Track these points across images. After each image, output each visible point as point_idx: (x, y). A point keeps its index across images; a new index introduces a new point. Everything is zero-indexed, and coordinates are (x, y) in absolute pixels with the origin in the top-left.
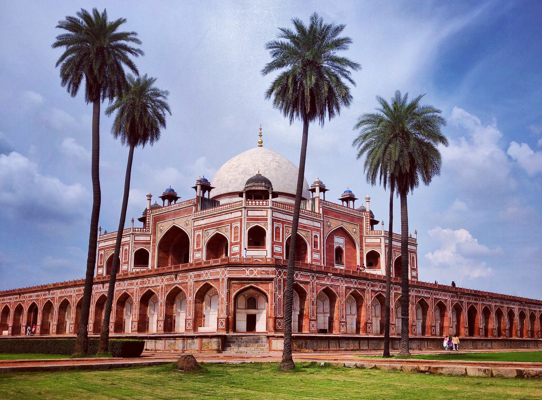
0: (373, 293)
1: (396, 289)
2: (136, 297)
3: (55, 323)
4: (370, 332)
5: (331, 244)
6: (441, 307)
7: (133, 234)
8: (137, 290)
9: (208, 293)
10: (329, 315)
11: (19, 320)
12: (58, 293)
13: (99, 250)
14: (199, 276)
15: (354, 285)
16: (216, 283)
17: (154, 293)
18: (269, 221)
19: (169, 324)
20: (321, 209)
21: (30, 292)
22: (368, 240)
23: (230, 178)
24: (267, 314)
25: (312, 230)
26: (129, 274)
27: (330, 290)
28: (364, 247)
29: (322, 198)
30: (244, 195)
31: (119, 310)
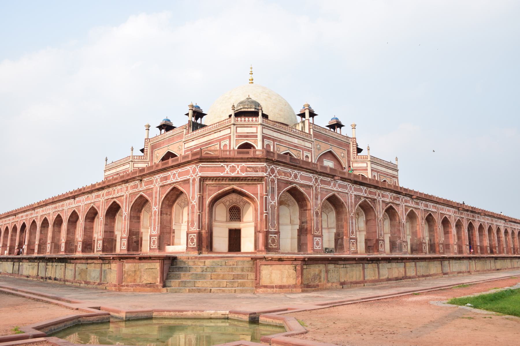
0: (384, 205)
2: (102, 210)
4: (382, 251)
7: (132, 161)
8: (103, 202)
10: (335, 231)
12: (40, 213)
14: (166, 178)
15: (364, 192)
16: (187, 185)
18: (260, 138)
20: (311, 130)
21: (22, 212)
22: (355, 165)
24: (256, 228)
25: (304, 150)
26: (97, 185)
29: (311, 121)
31: (88, 227)
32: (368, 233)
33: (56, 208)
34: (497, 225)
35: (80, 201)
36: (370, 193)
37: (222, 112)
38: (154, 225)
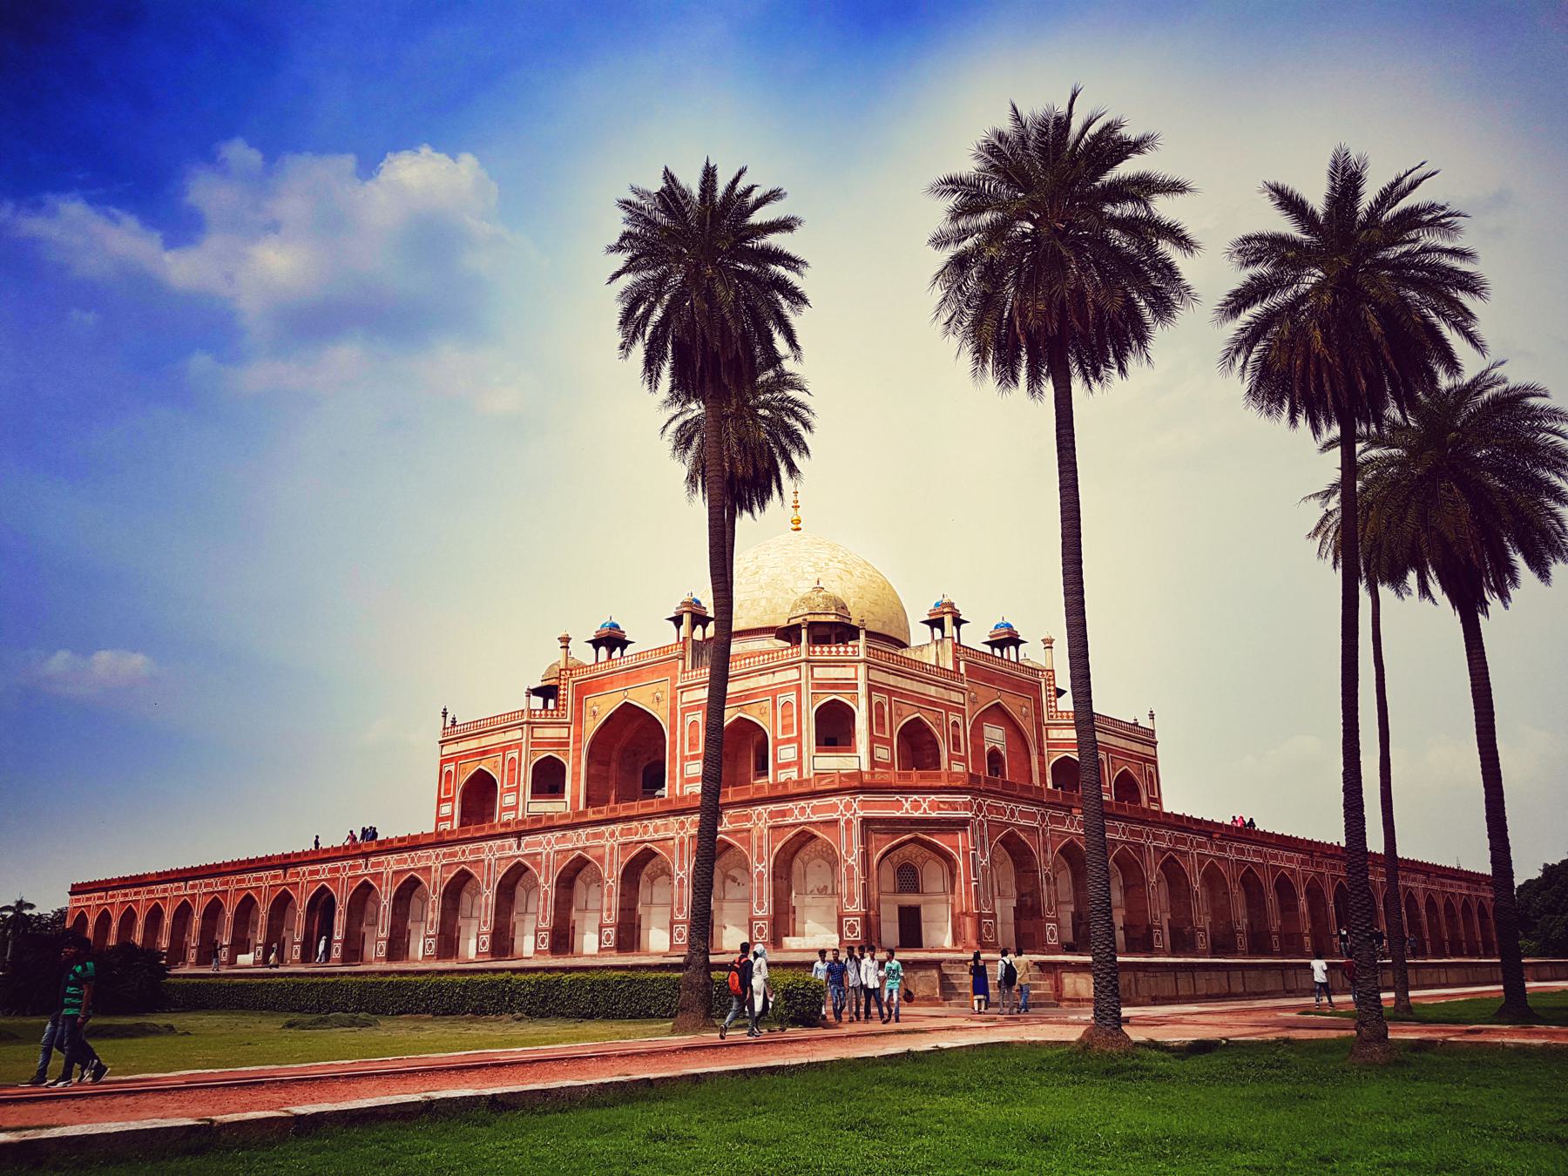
2: (611, 864)
3: (384, 935)
5: (978, 741)
6: (1284, 886)
7: (528, 723)
8: (612, 848)
9: (801, 854)
10: (1072, 908)
13: (442, 762)
14: (783, 814)
16: (831, 829)
17: (655, 854)
18: (862, 690)
25: (948, 709)
27: (1076, 846)
30: (804, 633)
33: (454, 855)
38: (760, 897)
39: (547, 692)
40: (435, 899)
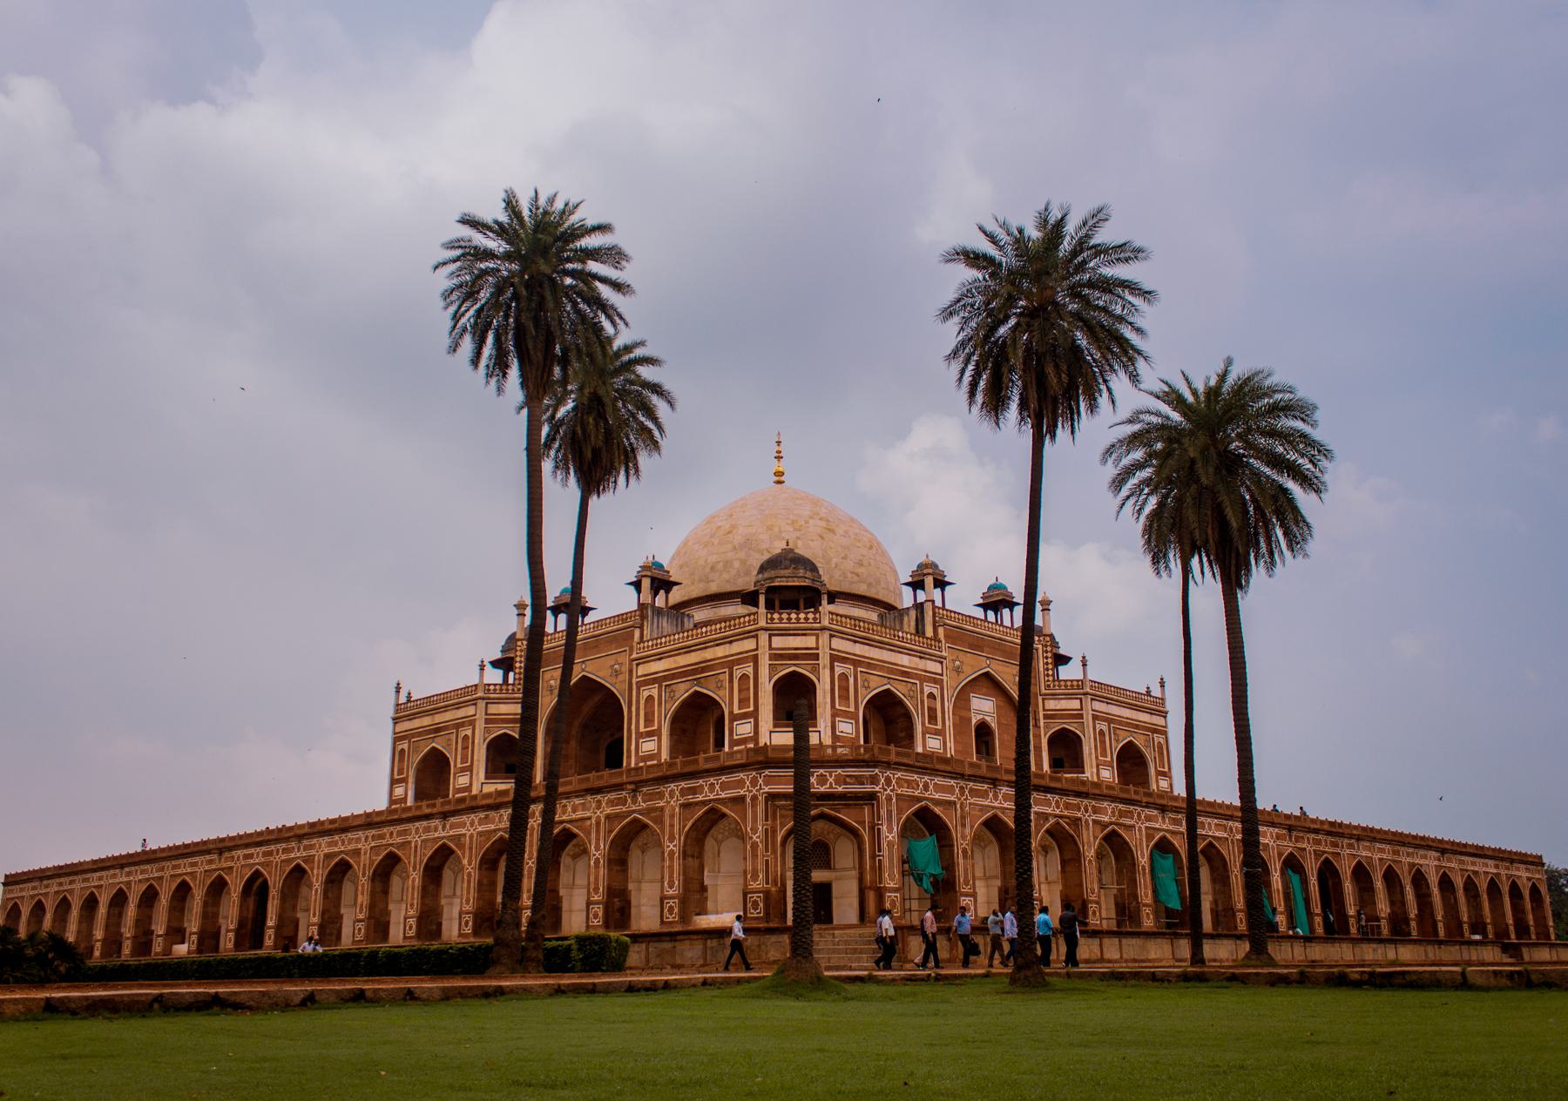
0: (1098, 828)
1: (1148, 819)
3: (315, 920)
5: (964, 713)
10: (998, 883)
11: (216, 915)
12: (323, 847)
14: (694, 791)
17: (575, 836)
18: (824, 660)
19: (618, 907)
21: (247, 846)
22: (1051, 704)
23: (712, 559)
24: (861, 880)
25: (923, 679)
28: (1042, 722)
30: (762, 599)
32: (1065, 886)
33: (382, 837)
34: (1412, 865)
35: (463, 825)
36: (1067, 806)
37: (712, 568)
38: (671, 876)
39: (504, 664)
40: (364, 881)
